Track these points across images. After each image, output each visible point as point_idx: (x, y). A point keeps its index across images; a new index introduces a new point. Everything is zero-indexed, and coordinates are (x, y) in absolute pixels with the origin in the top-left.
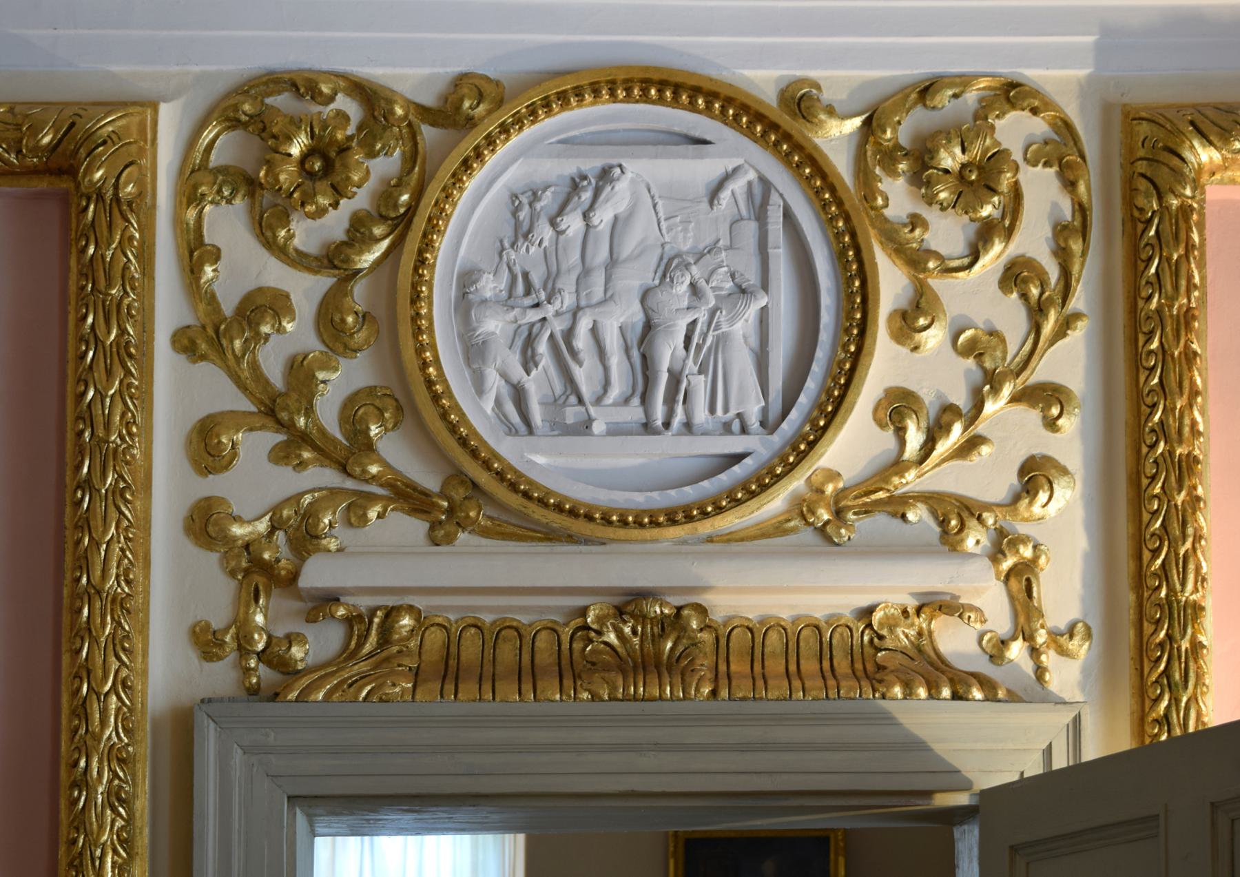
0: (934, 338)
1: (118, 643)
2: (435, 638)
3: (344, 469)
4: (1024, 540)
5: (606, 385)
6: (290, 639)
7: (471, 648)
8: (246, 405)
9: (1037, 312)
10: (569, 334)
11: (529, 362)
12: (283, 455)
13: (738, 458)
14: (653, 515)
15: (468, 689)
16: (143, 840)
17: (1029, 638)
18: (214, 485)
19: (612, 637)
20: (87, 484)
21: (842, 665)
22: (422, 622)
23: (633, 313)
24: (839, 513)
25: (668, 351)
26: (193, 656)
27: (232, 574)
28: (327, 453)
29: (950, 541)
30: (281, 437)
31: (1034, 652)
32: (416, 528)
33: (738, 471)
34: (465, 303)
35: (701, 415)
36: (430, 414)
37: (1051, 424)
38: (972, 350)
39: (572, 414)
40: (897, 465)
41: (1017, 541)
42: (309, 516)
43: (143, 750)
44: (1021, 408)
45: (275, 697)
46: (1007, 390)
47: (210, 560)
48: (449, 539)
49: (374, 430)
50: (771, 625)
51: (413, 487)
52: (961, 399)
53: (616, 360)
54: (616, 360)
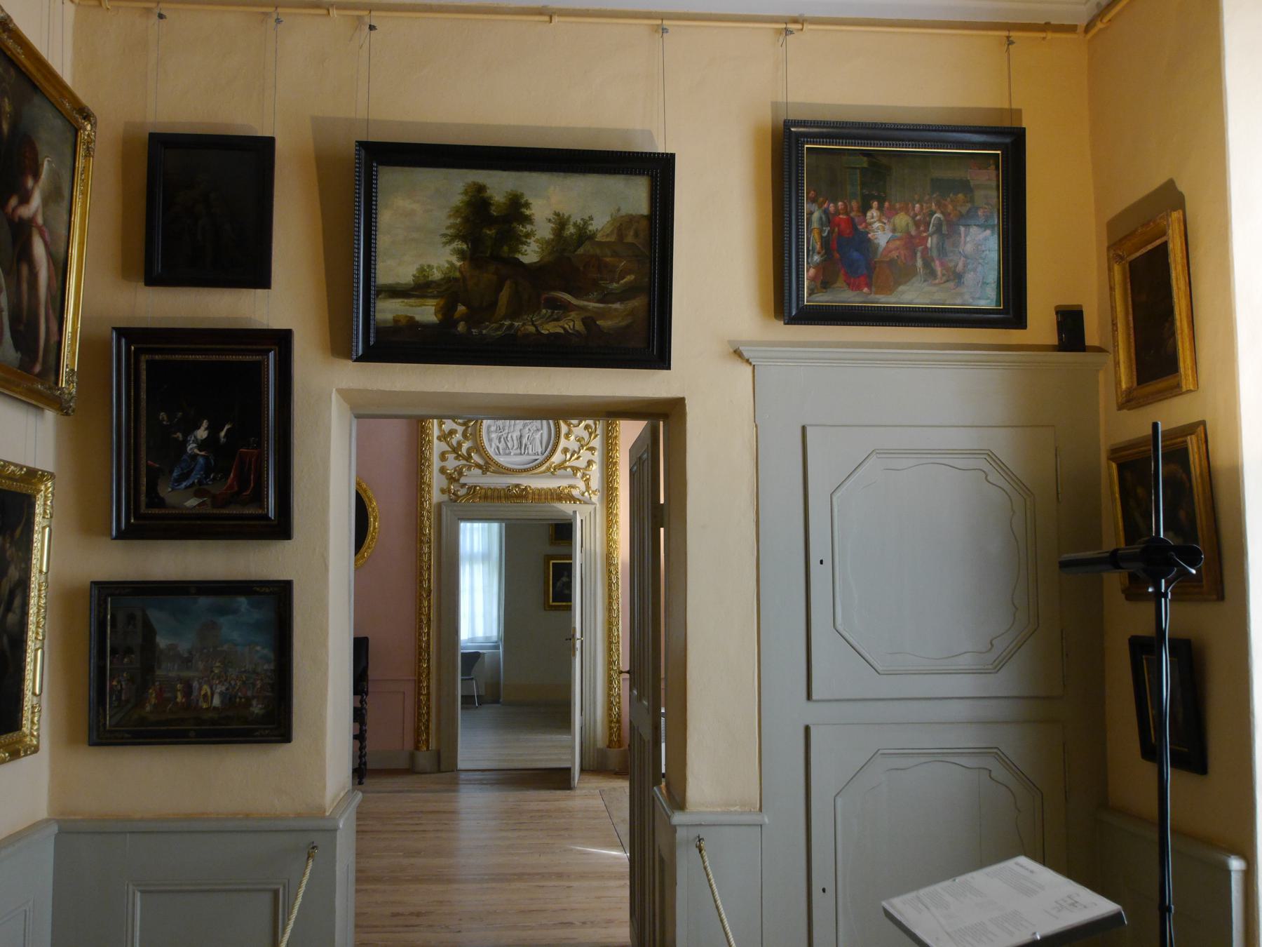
0: (572, 438)
1: (429, 492)
2: (483, 491)
3: (467, 461)
5: (513, 446)
6: (458, 491)
7: (489, 493)
8: (450, 450)
9: (590, 434)
10: (507, 437)
11: (500, 442)
12: (456, 458)
13: (536, 460)
15: (489, 500)
16: (432, 526)
20: (423, 464)
21: (555, 497)
22: (481, 488)
24: (555, 470)
26: (440, 493)
27: (447, 479)
29: (575, 475)
30: (456, 455)
31: (589, 494)
32: (480, 471)
33: (537, 462)
34: (489, 432)
35: (530, 452)
36: (482, 452)
37: (593, 454)
38: (578, 441)
39: (507, 451)
40: (565, 461)
41: (586, 475)
42: (461, 469)
43: (432, 510)
46: (585, 448)
49: (472, 454)
50: (542, 489)
51: (480, 464)
52: (577, 450)
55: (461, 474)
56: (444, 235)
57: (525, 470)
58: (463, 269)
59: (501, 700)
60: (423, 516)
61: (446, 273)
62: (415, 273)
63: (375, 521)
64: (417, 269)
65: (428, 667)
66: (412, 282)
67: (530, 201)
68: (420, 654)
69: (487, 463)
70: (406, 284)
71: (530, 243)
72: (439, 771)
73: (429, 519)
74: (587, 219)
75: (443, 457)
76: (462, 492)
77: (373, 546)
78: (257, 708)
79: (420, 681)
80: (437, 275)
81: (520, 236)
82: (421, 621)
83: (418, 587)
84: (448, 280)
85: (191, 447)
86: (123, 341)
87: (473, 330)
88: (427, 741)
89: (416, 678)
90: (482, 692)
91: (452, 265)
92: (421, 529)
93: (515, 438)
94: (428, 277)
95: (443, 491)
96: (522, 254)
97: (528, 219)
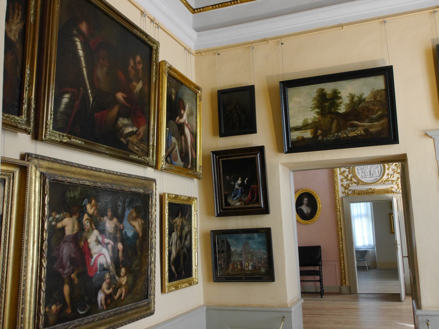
0: (390, 169)
2: (358, 192)
3: (351, 181)
4: (398, 183)
5: (368, 174)
6: (348, 192)
7: (360, 192)
8: (344, 178)
9: (397, 167)
10: (365, 171)
11: (362, 173)
13: (377, 179)
14: (372, 183)
15: (360, 195)
16: (340, 205)
17: (399, 189)
18: (342, 183)
19: (370, 191)
21: (386, 192)
22: (357, 191)
23: (369, 170)
24: (384, 182)
25: (372, 172)
26: (342, 194)
27: (344, 188)
28: (350, 180)
29: (393, 183)
31: (399, 190)
33: (377, 180)
34: (358, 170)
35: (374, 176)
38: (393, 170)
39: (366, 177)
40: (388, 178)
42: (349, 184)
43: (340, 200)
44: (397, 174)
45: (348, 196)
46: (396, 173)
47: (343, 188)
48: (358, 185)
49: (353, 179)
50: (381, 189)
52: (392, 174)
53: (368, 173)
54: (368, 173)
55: (349, 186)
56: (311, 108)
57: (373, 183)
58: (319, 118)
59: (377, 268)
60: (336, 202)
61: (313, 120)
62: (302, 122)
63: (319, 205)
64: (303, 120)
65: (343, 256)
66: (302, 125)
67: (340, 91)
68: (340, 251)
69: (358, 181)
70: (300, 126)
71: (341, 106)
72: (351, 294)
73: (339, 203)
74: (362, 94)
75: (342, 180)
76: (350, 192)
77: (320, 213)
78: (263, 270)
79: (341, 261)
80: (310, 121)
81: (338, 104)
82: (339, 239)
83: (337, 227)
84: (314, 122)
85: (237, 186)
86: (214, 155)
87: (324, 138)
88: (345, 282)
89: (339, 260)
90: (370, 265)
91: (315, 117)
92: (336, 207)
93: (368, 172)
94: (307, 122)
95: (343, 193)
96: (339, 110)
97: (340, 98)
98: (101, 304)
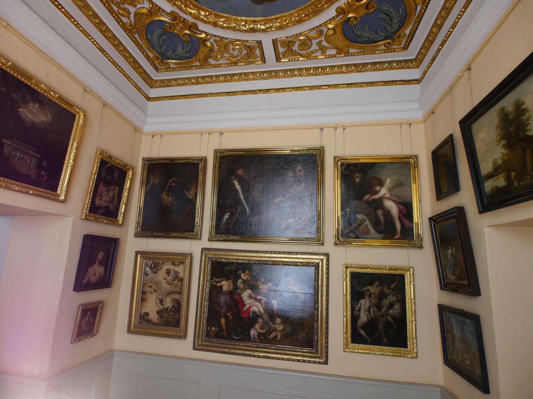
56: (497, 141)
58: (507, 154)
61: (503, 159)
62: (492, 165)
64: (493, 162)
66: (493, 170)
67: (523, 100)
71: (530, 123)
80: (499, 162)
81: (525, 122)
84: (504, 162)
87: (521, 183)
91: (503, 153)
94: (497, 164)
96: (529, 131)
97: (526, 110)
98: (254, 337)
